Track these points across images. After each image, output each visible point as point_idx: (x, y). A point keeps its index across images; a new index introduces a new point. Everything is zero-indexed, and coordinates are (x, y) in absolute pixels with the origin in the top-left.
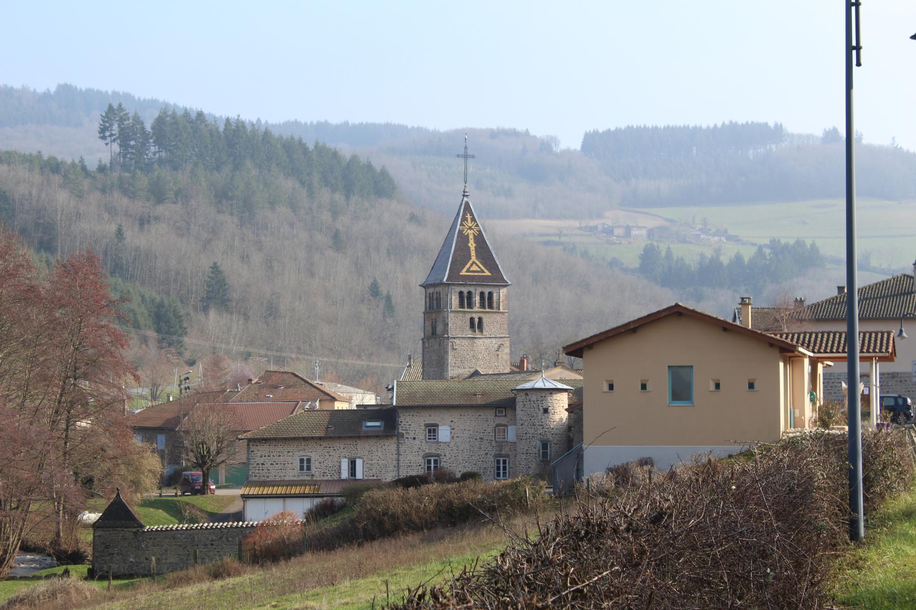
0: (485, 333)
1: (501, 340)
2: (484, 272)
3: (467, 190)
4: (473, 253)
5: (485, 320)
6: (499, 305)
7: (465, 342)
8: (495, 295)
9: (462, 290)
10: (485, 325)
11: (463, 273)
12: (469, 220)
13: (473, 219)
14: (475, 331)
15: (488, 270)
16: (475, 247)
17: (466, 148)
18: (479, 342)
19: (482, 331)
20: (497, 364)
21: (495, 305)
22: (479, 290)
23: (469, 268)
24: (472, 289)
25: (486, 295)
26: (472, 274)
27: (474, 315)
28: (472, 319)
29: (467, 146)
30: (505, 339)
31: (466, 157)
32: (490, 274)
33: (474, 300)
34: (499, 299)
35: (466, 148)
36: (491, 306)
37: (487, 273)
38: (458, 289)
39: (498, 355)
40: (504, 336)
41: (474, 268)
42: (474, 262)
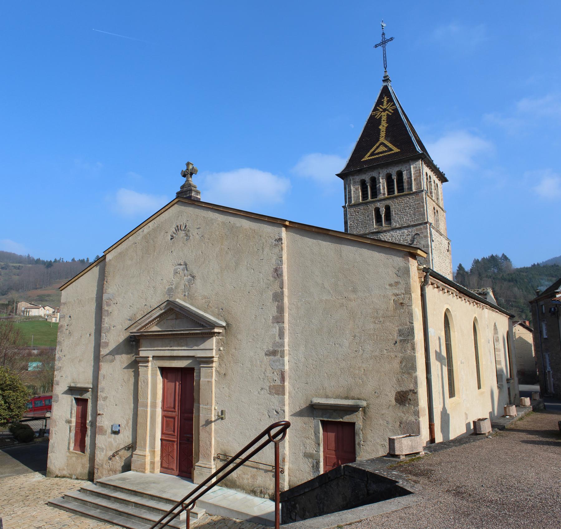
0: (394, 224)
1: (415, 228)
2: (393, 150)
4: (383, 134)
5: (392, 209)
6: (411, 184)
8: (405, 173)
11: (366, 158)
12: (385, 103)
13: (391, 100)
14: (382, 225)
15: (396, 146)
16: (387, 128)
17: (383, 34)
19: (390, 224)
21: (406, 186)
23: (374, 151)
24: (374, 174)
25: (395, 178)
26: (377, 156)
27: (378, 205)
28: (377, 211)
30: (422, 227)
31: (384, 43)
33: (377, 186)
34: (411, 178)
35: (383, 34)
36: (401, 189)
37: (396, 150)
38: (358, 178)
41: (382, 149)
42: (382, 144)
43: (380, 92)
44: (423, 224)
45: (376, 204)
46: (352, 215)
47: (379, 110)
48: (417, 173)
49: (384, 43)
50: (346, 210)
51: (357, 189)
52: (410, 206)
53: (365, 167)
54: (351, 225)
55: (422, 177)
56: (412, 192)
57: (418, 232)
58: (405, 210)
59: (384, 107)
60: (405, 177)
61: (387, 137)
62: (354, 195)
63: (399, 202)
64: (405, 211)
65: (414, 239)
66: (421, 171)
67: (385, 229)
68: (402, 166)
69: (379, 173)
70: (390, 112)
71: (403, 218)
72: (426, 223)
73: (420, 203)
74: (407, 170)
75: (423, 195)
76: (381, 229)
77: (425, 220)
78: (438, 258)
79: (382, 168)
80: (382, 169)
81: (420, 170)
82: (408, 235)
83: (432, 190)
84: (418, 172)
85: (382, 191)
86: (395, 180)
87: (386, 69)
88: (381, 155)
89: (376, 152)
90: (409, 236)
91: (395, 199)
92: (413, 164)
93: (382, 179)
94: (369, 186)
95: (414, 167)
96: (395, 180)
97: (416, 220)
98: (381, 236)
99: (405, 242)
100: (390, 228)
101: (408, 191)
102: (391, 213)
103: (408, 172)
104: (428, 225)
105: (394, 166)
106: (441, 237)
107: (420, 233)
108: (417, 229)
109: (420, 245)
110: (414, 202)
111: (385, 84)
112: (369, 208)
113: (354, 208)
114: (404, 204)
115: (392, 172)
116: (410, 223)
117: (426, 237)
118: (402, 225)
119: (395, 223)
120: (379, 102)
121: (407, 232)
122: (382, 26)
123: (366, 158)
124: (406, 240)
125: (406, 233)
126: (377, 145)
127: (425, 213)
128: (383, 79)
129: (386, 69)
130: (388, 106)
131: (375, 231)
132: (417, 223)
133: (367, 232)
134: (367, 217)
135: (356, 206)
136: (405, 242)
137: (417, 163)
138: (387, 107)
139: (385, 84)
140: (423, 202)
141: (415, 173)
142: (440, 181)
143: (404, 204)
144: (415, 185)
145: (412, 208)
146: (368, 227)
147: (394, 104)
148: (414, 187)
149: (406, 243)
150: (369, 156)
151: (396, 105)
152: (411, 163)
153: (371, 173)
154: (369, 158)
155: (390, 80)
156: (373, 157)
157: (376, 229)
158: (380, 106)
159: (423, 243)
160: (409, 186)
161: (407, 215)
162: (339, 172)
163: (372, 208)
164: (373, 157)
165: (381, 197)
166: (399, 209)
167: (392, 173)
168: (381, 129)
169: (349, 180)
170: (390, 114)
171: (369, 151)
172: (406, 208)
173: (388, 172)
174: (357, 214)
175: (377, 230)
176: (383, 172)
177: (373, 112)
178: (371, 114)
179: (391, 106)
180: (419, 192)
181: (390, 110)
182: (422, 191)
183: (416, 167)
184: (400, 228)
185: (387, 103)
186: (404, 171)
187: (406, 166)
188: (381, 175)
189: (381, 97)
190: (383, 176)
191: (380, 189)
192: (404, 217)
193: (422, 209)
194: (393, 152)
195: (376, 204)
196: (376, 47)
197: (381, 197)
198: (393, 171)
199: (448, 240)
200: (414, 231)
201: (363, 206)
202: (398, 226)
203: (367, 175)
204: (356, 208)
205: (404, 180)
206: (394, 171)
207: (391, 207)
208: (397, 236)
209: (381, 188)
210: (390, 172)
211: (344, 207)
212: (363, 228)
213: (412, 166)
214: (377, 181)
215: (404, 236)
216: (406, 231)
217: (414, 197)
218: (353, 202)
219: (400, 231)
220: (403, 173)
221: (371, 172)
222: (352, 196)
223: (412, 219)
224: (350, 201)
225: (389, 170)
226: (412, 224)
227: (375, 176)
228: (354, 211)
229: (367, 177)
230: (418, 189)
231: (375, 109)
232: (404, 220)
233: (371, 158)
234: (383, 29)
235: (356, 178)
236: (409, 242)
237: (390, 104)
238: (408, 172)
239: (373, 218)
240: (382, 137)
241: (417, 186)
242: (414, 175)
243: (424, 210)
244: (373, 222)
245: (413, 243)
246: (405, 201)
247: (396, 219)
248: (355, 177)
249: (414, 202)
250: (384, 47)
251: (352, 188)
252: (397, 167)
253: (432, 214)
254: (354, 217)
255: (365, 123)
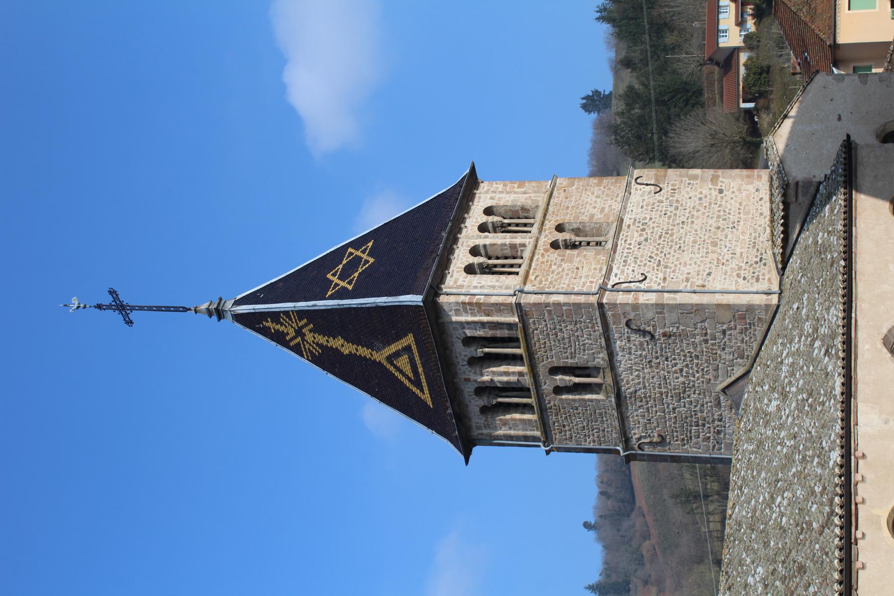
1: (613, 327)
3: (204, 306)
4: (363, 352)
7: (635, 414)
8: (469, 333)
9: (478, 409)
10: (570, 362)
11: (426, 397)
14: (599, 386)
17: (99, 307)
18: (629, 382)
20: (698, 339)
22: (464, 371)
24: (468, 390)
26: (423, 377)
29: (95, 304)
30: (609, 313)
31: (121, 308)
32: (411, 336)
33: (499, 385)
34: (483, 324)
35: (99, 307)
37: (409, 340)
38: (476, 419)
39: (664, 335)
40: (597, 313)
41: (403, 362)
42: (390, 359)
43: (248, 330)
44: (603, 311)
45: (545, 391)
46: (571, 438)
47: (299, 343)
48: (470, 310)
49: (121, 308)
50: (556, 448)
51: (505, 423)
52: (555, 329)
53: (450, 411)
54: (594, 441)
55: (482, 299)
56: (520, 325)
57: (624, 321)
58: (564, 338)
59: (292, 333)
60: (480, 333)
61: (369, 346)
62: (519, 430)
63: (543, 349)
64: (567, 341)
65: (639, 330)
66: (467, 299)
67: (609, 380)
68: (452, 336)
69: (468, 380)
70: (306, 325)
71: (584, 344)
72: (601, 305)
73: (550, 312)
74: (464, 328)
75: (529, 304)
76: (608, 387)
77: (591, 305)
78: (686, 257)
79: (455, 375)
80: (456, 373)
81: (464, 303)
82: (629, 341)
83: (505, 245)
84: (468, 307)
85: (513, 379)
86: (487, 350)
87: (190, 309)
88: (420, 370)
89: (411, 375)
90: (632, 339)
91: (536, 356)
92: (449, 315)
93: (482, 375)
94: (500, 400)
95: (456, 315)
96: (487, 350)
97: (592, 320)
98: (629, 391)
99: (645, 346)
100: (608, 371)
101: (517, 330)
102: (569, 365)
103: (466, 326)
104: (605, 301)
105: (452, 351)
106: (627, 221)
107: (625, 317)
108: (614, 323)
109: (656, 320)
110: (545, 321)
111: (229, 316)
112: (555, 405)
113: (553, 432)
114: (549, 340)
115: (465, 356)
116: (597, 333)
117: (636, 307)
118: (602, 348)
119: (597, 360)
120: (279, 338)
121: (622, 341)
122: (78, 307)
123: (426, 397)
124: (641, 344)
125: (623, 343)
126: (392, 369)
127: (574, 304)
128: (215, 318)
129: (190, 309)
130: (289, 324)
131: (613, 400)
132: (599, 320)
133: (616, 415)
134: (577, 409)
135: (548, 429)
136: (645, 346)
137: (446, 308)
138: (292, 327)
139: (229, 316)
140: (547, 305)
141: (471, 313)
142: (475, 194)
143: (549, 340)
144: (501, 316)
145: (560, 325)
146: (603, 410)
147: (286, 313)
148: (505, 317)
149: (648, 345)
150: (422, 391)
151: (287, 309)
152: (446, 319)
153: (466, 394)
154: (426, 391)
155: (219, 304)
156: (423, 380)
157: (607, 397)
158: (288, 338)
159: (650, 315)
160: (505, 326)
161: (578, 336)
162: (462, 457)
163: (552, 400)
164: (423, 380)
165: (527, 381)
166: (562, 350)
167: (470, 356)
168: (350, 352)
169: (480, 437)
170: (312, 326)
171: (408, 388)
172: (559, 337)
173: (466, 363)
174: (567, 428)
175: (613, 396)
176: (464, 373)
177: (302, 356)
178: (308, 359)
179: (291, 319)
180: (521, 311)
181: (300, 324)
182: (518, 305)
183: (456, 310)
184: (611, 355)
185: (282, 324)
186: (465, 333)
187: (451, 329)
188: (472, 377)
189: (265, 332)
190: (475, 373)
191: (508, 383)
192: (581, 343)
193: (564, 308)
194: (414, 347)
195: (545, 391)
196: (132, 323)
197: (527, 381)
198: (465, 353)
199: (631, 183)
200: (618, 330)
201: (548, 416)
202: (604, 355)
203: (470, 402)
204: (552, 428)
205: (489, 336)
206: (462, 353)
207: (556, 365)
208: (631, 360)
209: (505, 379)
210: (466, 359)
211: (548, 452)
212: (604, 419)
213: (454, 319)
214: (488, 385)
215: (630, 348)
216: (618, 342)
217: (531, 321)
218: (537, 433)
219: (617, 355)
220: (469, 335)
221: (462, 394)
222: (521, 433)
223: (588, 327)
224: (535, 439)
225: (459, 360)
226: (600, 328)
227: (474, 388)
228: (560, 433)
229: (475, 404)
230: (512, 311)
231: (297, 350)
232: (590, 342)
233: (425, 384)
234: (85, 307)
235: (478, 423)
236: (648, 339)
237: (283, 319)
238: (466, 326)
239: (580, 400)
240: (372, 355)
241: (505, 312)
242: (476, 316)
243: (565, 304)
244: (591, 400)
245: (649, 333)
246: (541, 337)
247: (585, 357)
248: (474, 425)
249: (545, 321)
250: (133, 308)
251: (500, 432)
252: (453, 345)
253: (571, 261)
254: (574, 435)
255: (330, 376)
